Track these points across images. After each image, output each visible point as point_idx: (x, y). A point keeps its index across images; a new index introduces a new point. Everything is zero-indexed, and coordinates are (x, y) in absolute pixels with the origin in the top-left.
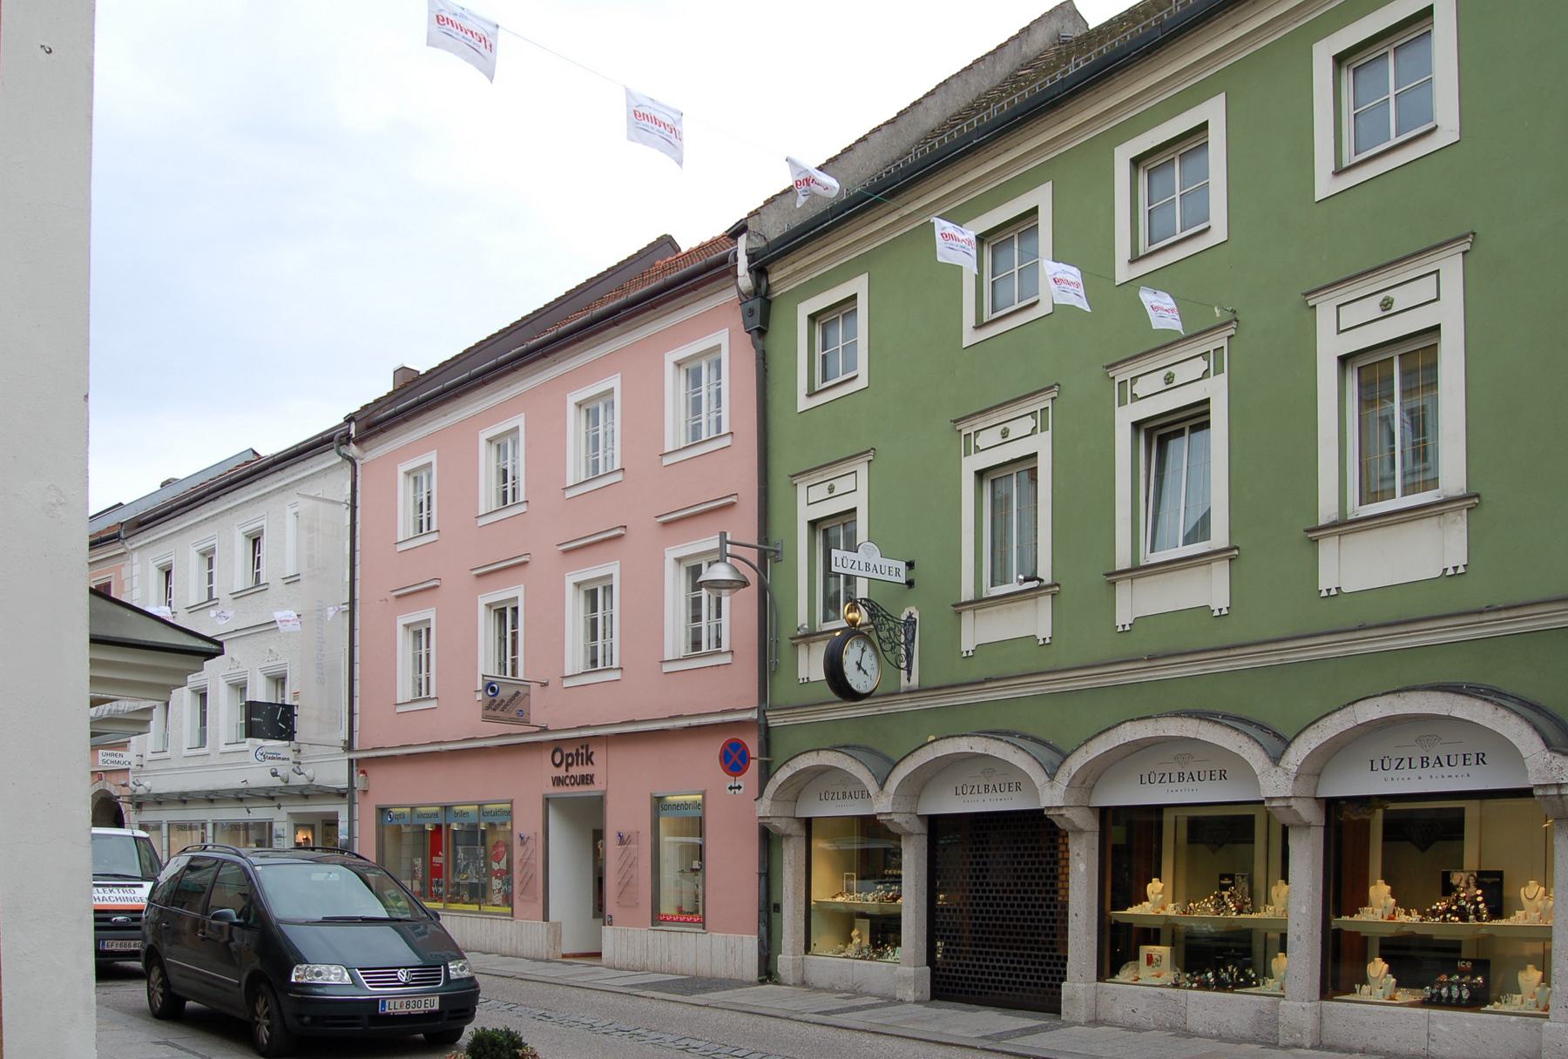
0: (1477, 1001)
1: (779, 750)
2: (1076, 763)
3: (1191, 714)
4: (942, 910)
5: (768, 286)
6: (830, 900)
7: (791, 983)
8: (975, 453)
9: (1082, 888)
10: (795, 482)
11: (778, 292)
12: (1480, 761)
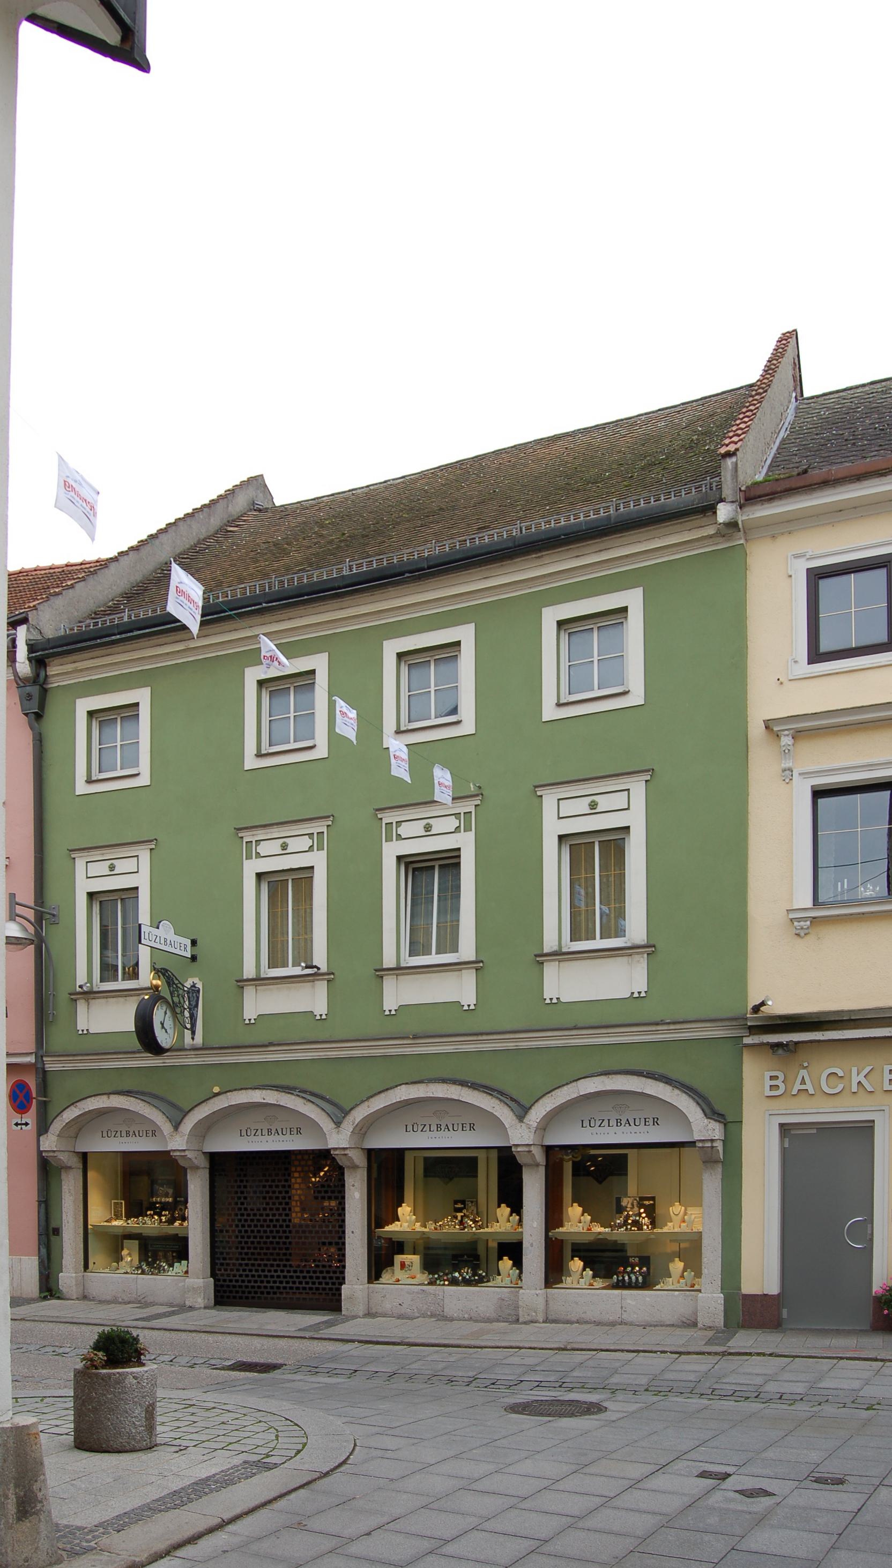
0: (647, 1284)
1: (57, 1094)
2: (359, 1114)
3: (463, 1084)
4: (221, 1231)
5: (46, 676)
6: (105, 1224)
7: (74, 1298)
8: (256, 858)
9: (357, 1211)
10: (73, 856)
11: (54, 684)
12: (655, 1124)
